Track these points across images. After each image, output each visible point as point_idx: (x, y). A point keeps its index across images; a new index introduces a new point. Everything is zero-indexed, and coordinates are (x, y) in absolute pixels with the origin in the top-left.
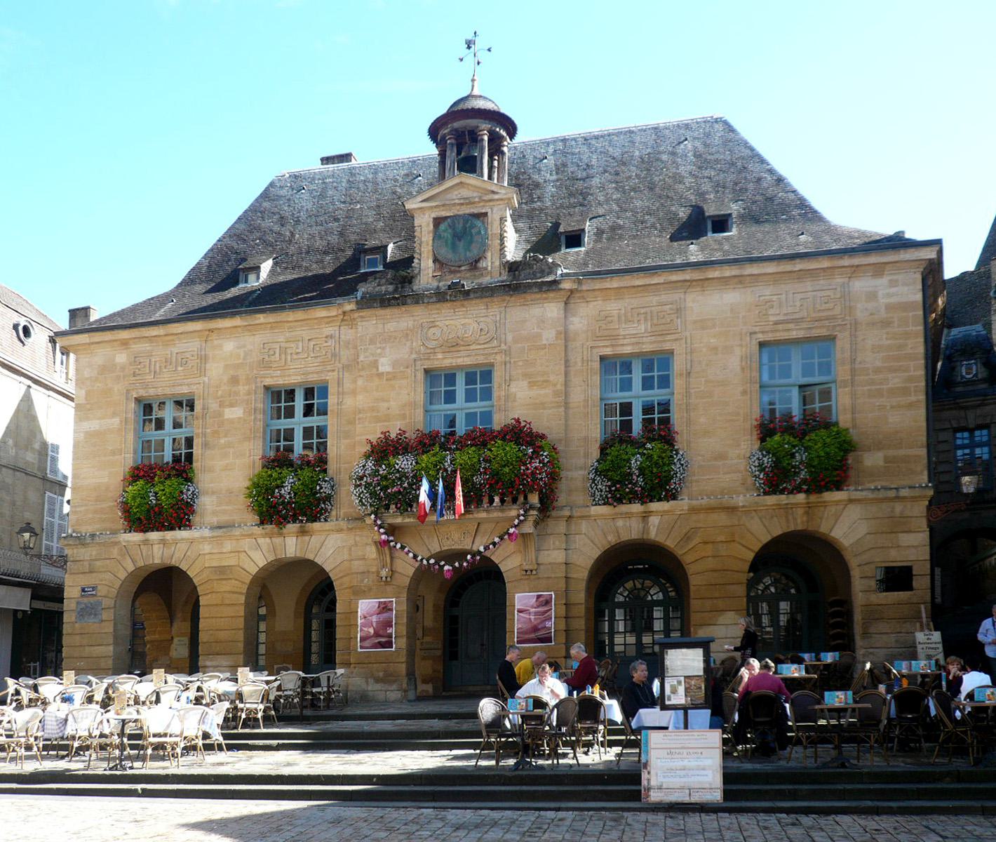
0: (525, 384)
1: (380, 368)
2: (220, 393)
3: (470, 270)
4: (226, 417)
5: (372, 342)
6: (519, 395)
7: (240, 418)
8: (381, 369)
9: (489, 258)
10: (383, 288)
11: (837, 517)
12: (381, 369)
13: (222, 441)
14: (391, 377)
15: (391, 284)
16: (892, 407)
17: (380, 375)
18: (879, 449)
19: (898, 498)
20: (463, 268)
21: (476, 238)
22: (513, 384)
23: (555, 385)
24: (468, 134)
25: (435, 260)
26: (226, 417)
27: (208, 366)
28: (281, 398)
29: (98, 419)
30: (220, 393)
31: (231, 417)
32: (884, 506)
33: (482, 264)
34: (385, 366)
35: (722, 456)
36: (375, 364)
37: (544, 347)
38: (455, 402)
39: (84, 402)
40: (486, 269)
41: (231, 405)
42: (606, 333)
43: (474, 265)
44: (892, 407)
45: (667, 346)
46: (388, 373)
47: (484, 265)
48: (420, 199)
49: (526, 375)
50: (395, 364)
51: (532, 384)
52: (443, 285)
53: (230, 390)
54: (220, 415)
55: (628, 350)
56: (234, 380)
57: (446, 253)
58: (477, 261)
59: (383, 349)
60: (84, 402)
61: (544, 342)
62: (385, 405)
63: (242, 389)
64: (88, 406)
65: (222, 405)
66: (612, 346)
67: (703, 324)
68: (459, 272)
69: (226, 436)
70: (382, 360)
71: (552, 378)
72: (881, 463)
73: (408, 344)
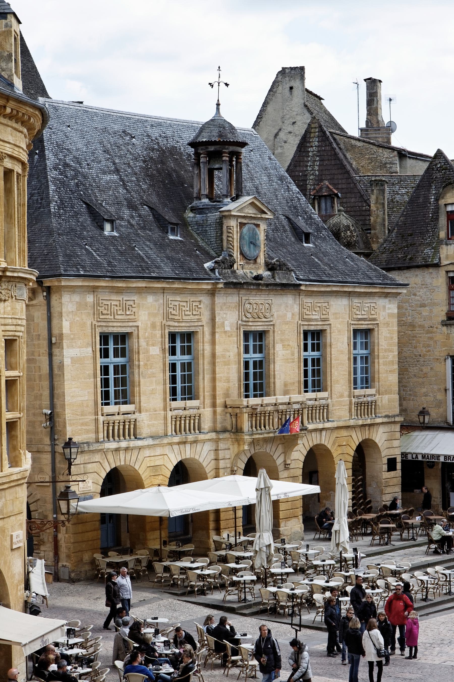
1: (226, 328)
4: (151, 354)
6: (280, 353)
7: (158, 355)
10: (226, 271)
17: (225, 332)
18: (386, 394)
19: (394, 422)
20: (251, 261)
25: (241, 253)
29: (80, 347)
30: (147, 334)
33: (258, 260)
37: (287, 323)
45: (325, 327)
50: (231, 326)
53: (152, 333)
56: (153, 326)
64: (72, 336)
65: (147, 344)
66: (309, 325)
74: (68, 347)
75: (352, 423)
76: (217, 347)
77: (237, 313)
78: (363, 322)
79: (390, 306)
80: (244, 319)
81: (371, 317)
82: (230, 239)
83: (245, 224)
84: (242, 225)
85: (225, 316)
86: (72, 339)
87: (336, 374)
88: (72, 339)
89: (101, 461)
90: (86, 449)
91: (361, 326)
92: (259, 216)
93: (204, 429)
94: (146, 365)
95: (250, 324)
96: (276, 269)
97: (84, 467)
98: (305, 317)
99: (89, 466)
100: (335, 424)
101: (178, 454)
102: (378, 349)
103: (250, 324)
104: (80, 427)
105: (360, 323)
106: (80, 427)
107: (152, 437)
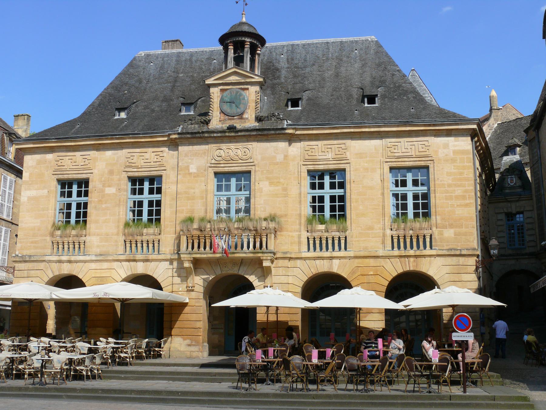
0: (267, 183)
2: (103, 179)
3: (239, 119)
4: (106, 192)
5: (186, 155)
7: (114, 194)
8: (191, 171)
9: (249, 113)
10: (193, 126)
11: (430, 263)
12: (191, 171)
13: (104, 206)
14: (196, 175)
15: (197, 124)
16: (457, 206)
17: (190, 174)
18: (452, 228)
20: (235, 117)
21: (242, 102)
22: (261, 183)
23: (283, 185)
24: (241, 42)
25: (222, 112)
26: (106, 192)
27: (97, 164)
28: (136, 182)
29: (36, 190)
30: (103, 179)
31: (109, 192)
32: (454, 258)
33: (245, 116)
34: (193, 169)
35: (371, 228)
36: (187, 168)
38: (230, 191)
39: (28, 180)
40: (247, 119)
41: (109, 186)
42: (310, 158)
43: (241, 116)
44: (457, 206)
45: (342, 166)
46: (195, 173)
47: (247, 117)
48: (213, 79)
49: (268, 178)
51: (271, 184)
52: (225, 126)
54: (103, 191)
55: (321, 167)
56: (111, 172)
57: (226, 108)
58: (242, 114)
59: (192, 159)
60: (28, 180)
61: (278, 161)
62: (193, 191)
63: (115, 177)
64: (30, 182)
65: (103, 186)
67: (360, 155)
68: (233, 119)
69: (106, 203)
70: (191, 166)
71: (282, 180)
72: (453, 236)
73: (206, 158)
74: (25, 190)
75: (381, 253)
76: (179, 186)
77: (206, 158)
78: (406, 159)
79: (457, 143)
80: (213, 161)
81: (418, 154)
82: (211, 103)
83: (227, 90)
84: (222, 90)
85: (190, 161)
86: (30, 184)
87: (361, 207)
88: (30, 184)
89: (44, 269)
90: (27, 260)
91: (403, 163)
92: (243, 81)
93: (162, 251)
94: (100, 201)
95: (222, 165)
96: (262, 121)
97: (28, 273)
98: (307, 157)
99: (33, 272)
100: (352, 254)
101: (128, 269)
102: (435, 185)
103: (222, 165)
104: (29, 244)
105: (400, 160)
106: (29, 244)
107: (96, 255)
